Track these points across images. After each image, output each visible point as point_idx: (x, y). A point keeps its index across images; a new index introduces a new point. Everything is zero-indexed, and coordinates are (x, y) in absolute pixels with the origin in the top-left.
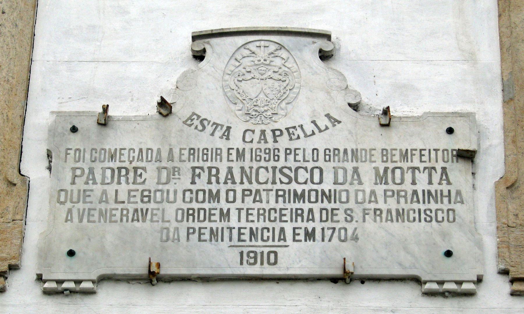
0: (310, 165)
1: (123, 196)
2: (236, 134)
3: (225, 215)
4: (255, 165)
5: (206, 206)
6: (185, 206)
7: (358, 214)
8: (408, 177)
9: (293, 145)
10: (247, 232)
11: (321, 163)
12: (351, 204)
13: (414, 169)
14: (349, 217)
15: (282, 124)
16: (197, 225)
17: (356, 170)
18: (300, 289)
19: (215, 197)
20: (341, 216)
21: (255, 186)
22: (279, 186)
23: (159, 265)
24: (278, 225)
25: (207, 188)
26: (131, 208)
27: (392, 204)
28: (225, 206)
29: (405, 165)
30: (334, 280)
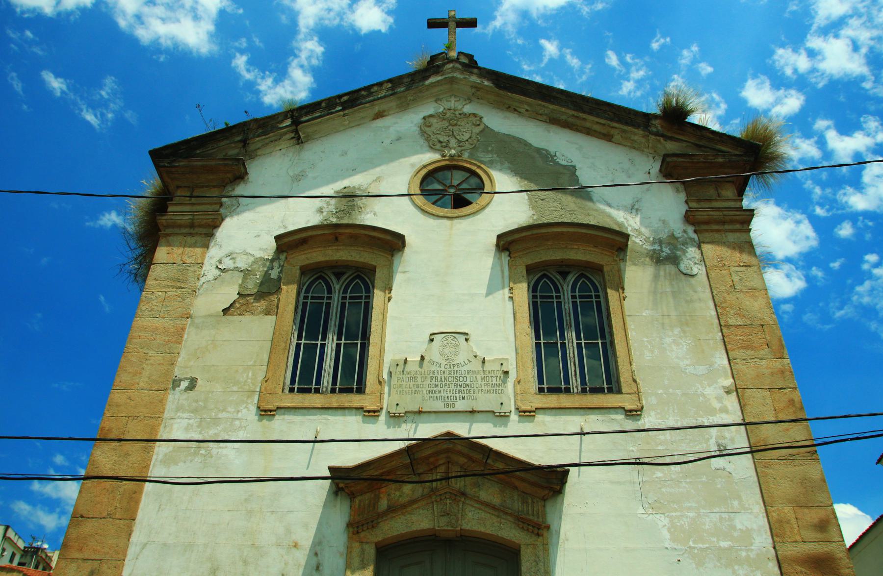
0: (463, 376)
1: (411, 386)
2: (443, 366)
3: (440, 392)
4: (448, 376)
5: (435, 389)
6: (429, 389)
7: (477, 391)
8: (490, 379)
9: (459, 369)
10: (446, 397)
11: (466, 375)
12: (475, 388)
13: (492, 376)
14: (474, 392)
15: (455, 362)
16: (432, 395)
17: (476, 377)
18: (461, 414)
19: (437, 386)
20: (472, 392)
21: (448, 383)
22: (455, 382)
23: (422, 408)
24: (454, 395)
25: (435, 383)
26: (414, 390)
27: (486, 388)
28: (440, 389)
29: (490, 375)
30: (470, 412)
